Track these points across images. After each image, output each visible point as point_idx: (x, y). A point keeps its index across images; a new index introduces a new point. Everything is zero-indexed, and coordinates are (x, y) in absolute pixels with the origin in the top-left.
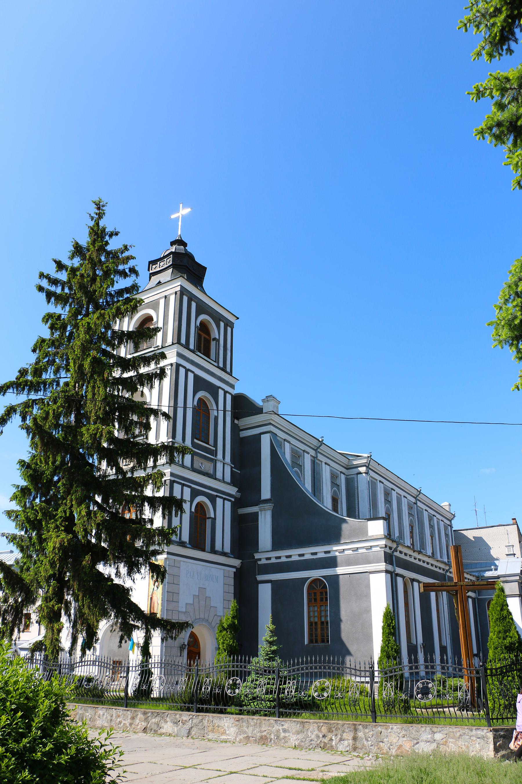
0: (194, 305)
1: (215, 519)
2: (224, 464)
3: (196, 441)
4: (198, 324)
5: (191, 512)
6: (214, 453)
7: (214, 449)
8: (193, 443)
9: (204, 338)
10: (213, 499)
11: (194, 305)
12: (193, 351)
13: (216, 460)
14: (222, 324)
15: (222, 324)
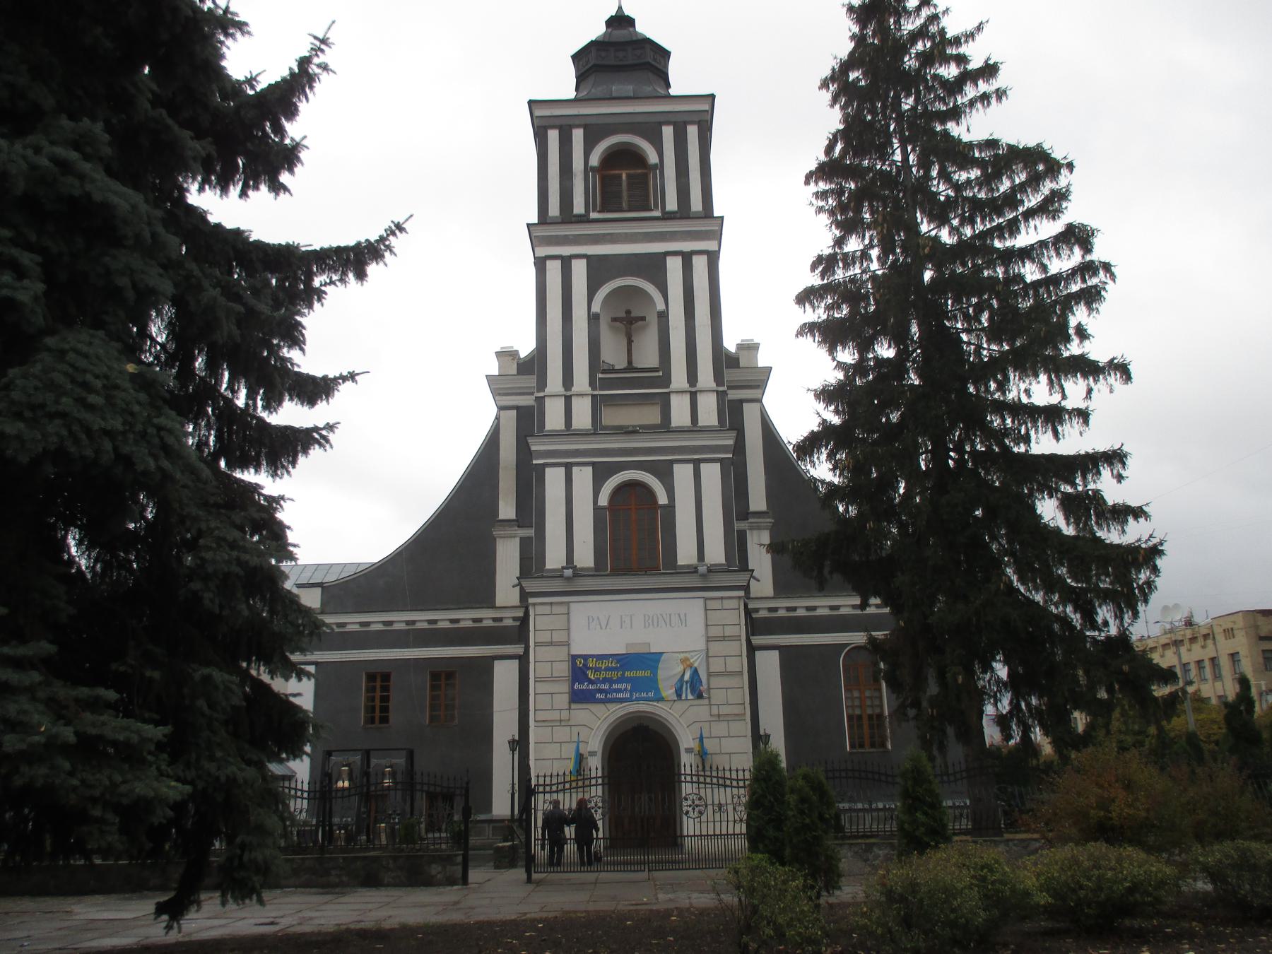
0: (578, 135)
1: (670, 508)
2: (693, 395)
3: (600, 376)
4: (595, 160)
5: (597, 509)
6: (666, 380)
7: (661, 374)
8: (592, 384)
9: (628, 176)
10: (664, 473)
11: (578, 135)
12: (583, 219)
13: (668, 394)
14: (668, 132)
15: (668, 132)
